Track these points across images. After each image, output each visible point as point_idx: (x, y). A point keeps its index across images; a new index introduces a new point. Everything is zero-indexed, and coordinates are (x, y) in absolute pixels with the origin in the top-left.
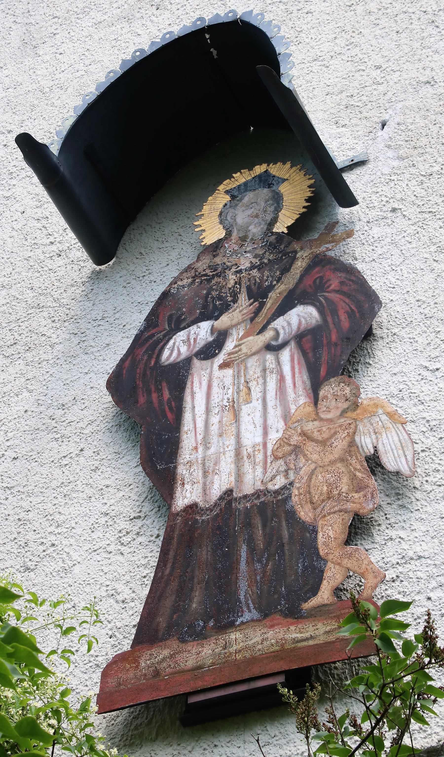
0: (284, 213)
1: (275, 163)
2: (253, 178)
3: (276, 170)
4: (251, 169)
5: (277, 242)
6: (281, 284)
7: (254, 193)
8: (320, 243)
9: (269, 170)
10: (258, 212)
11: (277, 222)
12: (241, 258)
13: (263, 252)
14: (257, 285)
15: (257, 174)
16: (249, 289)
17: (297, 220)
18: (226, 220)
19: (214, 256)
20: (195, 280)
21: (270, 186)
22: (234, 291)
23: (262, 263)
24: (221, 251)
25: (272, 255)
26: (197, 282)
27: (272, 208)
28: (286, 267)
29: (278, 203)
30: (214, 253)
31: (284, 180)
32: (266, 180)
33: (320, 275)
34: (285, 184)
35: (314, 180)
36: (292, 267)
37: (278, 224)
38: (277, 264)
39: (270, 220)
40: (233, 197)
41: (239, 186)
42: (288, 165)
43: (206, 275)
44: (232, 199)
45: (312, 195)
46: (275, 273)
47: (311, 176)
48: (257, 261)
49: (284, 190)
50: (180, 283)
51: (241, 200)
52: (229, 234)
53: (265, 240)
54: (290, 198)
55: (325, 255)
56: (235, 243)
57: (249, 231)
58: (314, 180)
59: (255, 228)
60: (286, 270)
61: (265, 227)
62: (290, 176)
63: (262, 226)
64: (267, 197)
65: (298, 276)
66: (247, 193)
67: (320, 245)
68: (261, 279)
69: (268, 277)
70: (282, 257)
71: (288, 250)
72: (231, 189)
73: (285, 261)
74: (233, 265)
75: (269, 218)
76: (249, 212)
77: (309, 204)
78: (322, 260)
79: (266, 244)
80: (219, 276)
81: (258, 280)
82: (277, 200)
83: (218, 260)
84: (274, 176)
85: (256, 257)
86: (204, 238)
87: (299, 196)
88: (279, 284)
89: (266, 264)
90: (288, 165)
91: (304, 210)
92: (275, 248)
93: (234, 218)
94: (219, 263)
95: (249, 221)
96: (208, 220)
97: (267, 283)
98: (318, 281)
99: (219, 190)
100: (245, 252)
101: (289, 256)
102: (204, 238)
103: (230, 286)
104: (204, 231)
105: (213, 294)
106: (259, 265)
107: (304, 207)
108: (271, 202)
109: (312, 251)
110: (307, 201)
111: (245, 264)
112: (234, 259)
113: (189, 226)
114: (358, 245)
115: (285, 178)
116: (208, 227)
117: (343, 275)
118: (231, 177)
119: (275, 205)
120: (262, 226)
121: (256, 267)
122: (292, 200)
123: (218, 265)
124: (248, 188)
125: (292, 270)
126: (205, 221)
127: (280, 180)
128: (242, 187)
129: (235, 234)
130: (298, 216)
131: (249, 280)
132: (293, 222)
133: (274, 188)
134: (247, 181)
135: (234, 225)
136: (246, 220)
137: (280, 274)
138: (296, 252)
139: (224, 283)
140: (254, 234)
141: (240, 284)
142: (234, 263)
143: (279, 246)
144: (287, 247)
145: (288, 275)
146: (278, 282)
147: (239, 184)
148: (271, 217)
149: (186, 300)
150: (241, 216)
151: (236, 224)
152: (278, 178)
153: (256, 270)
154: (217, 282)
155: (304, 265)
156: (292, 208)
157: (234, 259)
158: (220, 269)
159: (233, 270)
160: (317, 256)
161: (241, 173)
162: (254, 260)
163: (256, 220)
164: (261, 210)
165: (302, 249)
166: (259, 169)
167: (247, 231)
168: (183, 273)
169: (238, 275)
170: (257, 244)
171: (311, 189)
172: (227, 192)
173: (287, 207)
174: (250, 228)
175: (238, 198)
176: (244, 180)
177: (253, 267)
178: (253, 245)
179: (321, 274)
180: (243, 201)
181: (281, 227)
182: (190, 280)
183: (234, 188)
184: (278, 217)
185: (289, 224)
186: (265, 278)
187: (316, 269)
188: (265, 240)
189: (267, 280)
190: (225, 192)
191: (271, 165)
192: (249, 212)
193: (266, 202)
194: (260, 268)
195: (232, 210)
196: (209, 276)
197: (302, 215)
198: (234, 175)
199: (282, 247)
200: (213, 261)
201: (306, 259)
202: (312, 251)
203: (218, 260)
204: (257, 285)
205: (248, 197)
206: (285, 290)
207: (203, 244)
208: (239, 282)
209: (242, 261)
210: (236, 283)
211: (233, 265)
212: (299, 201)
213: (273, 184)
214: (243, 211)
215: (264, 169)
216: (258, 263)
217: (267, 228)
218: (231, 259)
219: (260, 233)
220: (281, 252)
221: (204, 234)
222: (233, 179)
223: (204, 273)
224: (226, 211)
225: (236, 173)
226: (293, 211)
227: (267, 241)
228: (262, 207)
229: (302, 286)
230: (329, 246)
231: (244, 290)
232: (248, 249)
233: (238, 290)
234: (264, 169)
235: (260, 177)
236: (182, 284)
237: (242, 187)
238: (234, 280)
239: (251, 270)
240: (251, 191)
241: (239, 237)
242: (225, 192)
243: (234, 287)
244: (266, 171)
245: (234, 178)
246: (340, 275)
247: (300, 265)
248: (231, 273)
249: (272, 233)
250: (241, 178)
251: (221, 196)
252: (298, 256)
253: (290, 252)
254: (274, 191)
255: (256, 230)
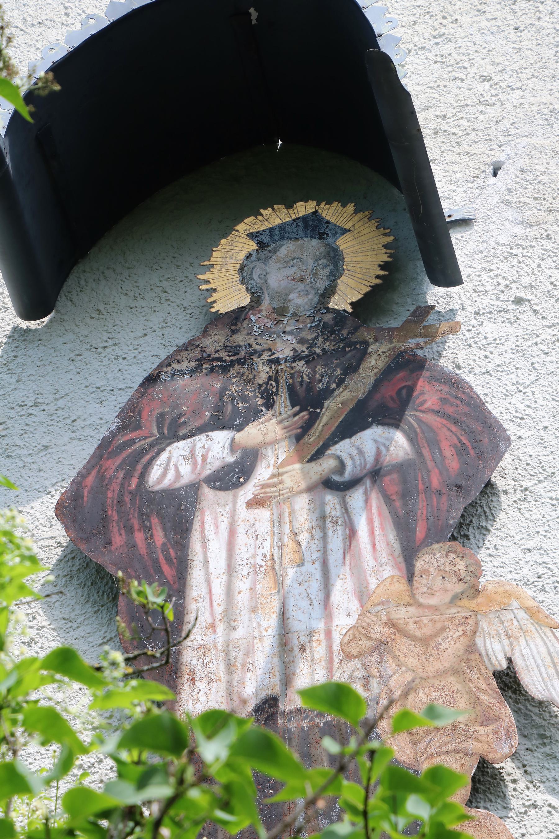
0: (345, 281)
1: (329, 203)
2: (294, 220)
3: (331, 212)
4: (289, 206)
5: (336, 324)
6: (344, 390)
7: (296, 243)
8: (406, 335)
9: (320, 211)
10: (303, 273)
11: (334, 293)
12: (278, 340)
13: (313, 336)
14: (304, 386)
15: (301, 215)
16: (291, 390)
17: (366, 295)
18: (252, 279)
19: (233, 332)
20: (202, 365)
21: (321, 236)
22: (266, 390)
23: (312, 354)
24: (245, 325)
25: (328, 344)
26: (206, 369)
27: (327, 271)
28: (352, 364)
29: (336, 265)
30: (233, 328)
31: (345, 231)
32: (314, 226)
33: (407, 384)
34: (347, 236)
35: (392, 238)
36: (362, 366)
37: (336, 296)
38: (337, 359)
39: (323, 288)
40: (262, 245)
41: (271, 230)
42: (351, 208)
43: (220, 359)
44: (260, 247)
45: (390, 260)
46: (334, 370)
47: (388, 231)
48: (304, 349)
49: (345, 246)
50: (176, 366)
51: (275, 251)
52: (256, 301)
53: (316, 319)
54: (354, 259)
55: (414, 355)
56: (266, 317)
57: (290, 301)
58: (392, 238)
59: (298, 297)
60: (352, 369)
61: (316, 299)
62: (353, 226)
63: (310, 296)
64: (318, 253)
65: (372, 380)
66: (285, 242)
67: (406, 338)
68: (312, 377)
69: (322, 376)
70: (344, 348)
71: (354, 339)
72: (258, 232)
73: (350, 354)
74: (264, 350)
75: (322, 285)
76: (290, 272)
77: (386, 273)
78: (409, 362)
79: (318, 325)
80: (243, 364)
81: (305, 378)
82: (335, 258)
83: (240, 339)
84: (328, 222)
85: (302, 341)
86: (215, 302)
87: (369, 259)
88: (341, 389)
89: (318, 356)
90: (351, 208)
91: (378, 281)
92: (332, 332)
93: (265, 277)
94: (242, 343)
95: (289, 285)
96: (220, 274)
97: (320, 385)
98: (404, 392)
99: (237, 231)
100: (284, 332)
101: (355, 347)
102: (215, 302)
103: (261, 382)
104: (214, 290)
105: (233, 390)
106: (307, 356)
107: (378, 277)
108: (324, 261)
109: (393, 345)
110: (382, 267)
111: (284, 350)
112: (265, 341)
113: (179, 280)
114: (462, 347)
115: (347, 227)
116: (222, 285)
117: (446, 389)
118: (257, 214)
119: (332, 267)
120: (310, 296)
121: (302, 358)
122: (358, 262)
123: (240, 346)
124: (287, 235)
125: (361, 370)
126: (216, 275)
127: (337, 229)
128: (277, 232)
129: (266, 303)
130: (369, 289)
131: (292, 376)
132: (360, 296)
133: (329, 240)
134: (285, 223)
135: (264, 288)
136: (284, 284)
137: (342, 374)
138: (367, 344)
139: (251, 376)
140: (298, 307)
141: (277, 381)
142: (266, 346)
143: (339, 331)
144: (352, 334)
145: (355, 376)
146: (339, 385)
147: (270, 226)
148: (324, 285)
149: (186, 394)
150: (276, 277)
151: (268, 287)
152: (335, 225)
153: (302, 363)
154: (238, 373)
155: (381, 365)
156: (359, 276)
157: (265, 341)
158: (243, 354)
159: (265, 356)
160: (401, 354)
161: (274, 209)
162: (299, 347)
163: (301, 286)
164: (309, 271)
165: (376, 340)
166: (303, 209)
167: (286, 301)
168: (181, 351)
169: (273, 366)
170: (303, 323)
171: (388, 251)
172: (251, 236)
173: (351, 273)
174: (291, 297)
175: (269, 248)
176: (278, 222)
177: (297, 357)
178: (297, 324)
179: (409, 383)
180: (278, 253)
181: (342, 301)
182: (193, 364)
183: (264, 231)
184: (336, 286)
185: (354, 300)
186: (318, 376)
187: (401, 375)
188: (316, 319)
189: (321, 381)
190: (248, 235)
191: (323, 204)
192: (290, 272)
193: (316, 260)
194: (309, 359)
195: (259, 265)
196: (225, 361)
197: (375, 289)
198: (262, 211)
199: (345, 332)
200: (231, 339)
201: (383, 357)
202: (393, 345)
203: (240, 339)
204: (304, 386)
205: (287, 249)
206: (352, 399)
207: (213, 310)
208: (275, 377)
209: (280, 345)
210: (270, 378)
211: (264, 350)
212: (370, 267)
213: (327, 235)
214: (279, 269)
215: (311, 208)
216: (306, 353)
217: (319, 301)
218: (260, 340)
219: (307, 307)
220: (343, 340)
221: (215, 296)
222: (260, 218)
223: (217, 355)
224: (251, 266)
225: (265, 209)
226: (360, 281)
227: (320, 321)
228: (310, 267)
229: (378, 396)
230: (421, 341)
231: (283, 390)
232: (288, 329)
233: (274, 390)
234: (311, 208)
235: (305, 219)
236: (180, 369)
237: (277, 232)
238: (267, 373)
239: (295, 361)
240: (290, 239)
241: (274, 309)
242: (248, 235)
243: (267, 384)
244: (315, 213)
245: (262, 215)
246: (440, 388)
247: (374, 364)
248: (261, 362)
249: (328, 309)
250: (274, 217)
251: (242, 240)
252: (370, 350)
253: (357, 343)
254: (328, 245)
255: (301, 300)
